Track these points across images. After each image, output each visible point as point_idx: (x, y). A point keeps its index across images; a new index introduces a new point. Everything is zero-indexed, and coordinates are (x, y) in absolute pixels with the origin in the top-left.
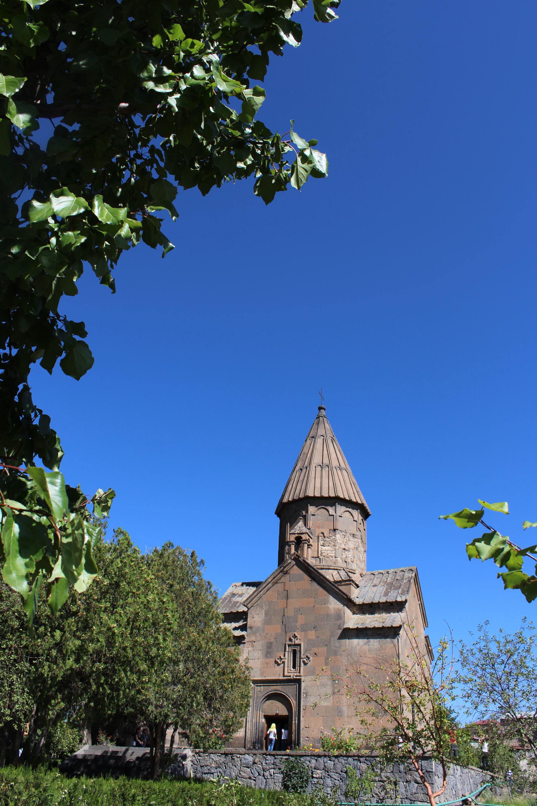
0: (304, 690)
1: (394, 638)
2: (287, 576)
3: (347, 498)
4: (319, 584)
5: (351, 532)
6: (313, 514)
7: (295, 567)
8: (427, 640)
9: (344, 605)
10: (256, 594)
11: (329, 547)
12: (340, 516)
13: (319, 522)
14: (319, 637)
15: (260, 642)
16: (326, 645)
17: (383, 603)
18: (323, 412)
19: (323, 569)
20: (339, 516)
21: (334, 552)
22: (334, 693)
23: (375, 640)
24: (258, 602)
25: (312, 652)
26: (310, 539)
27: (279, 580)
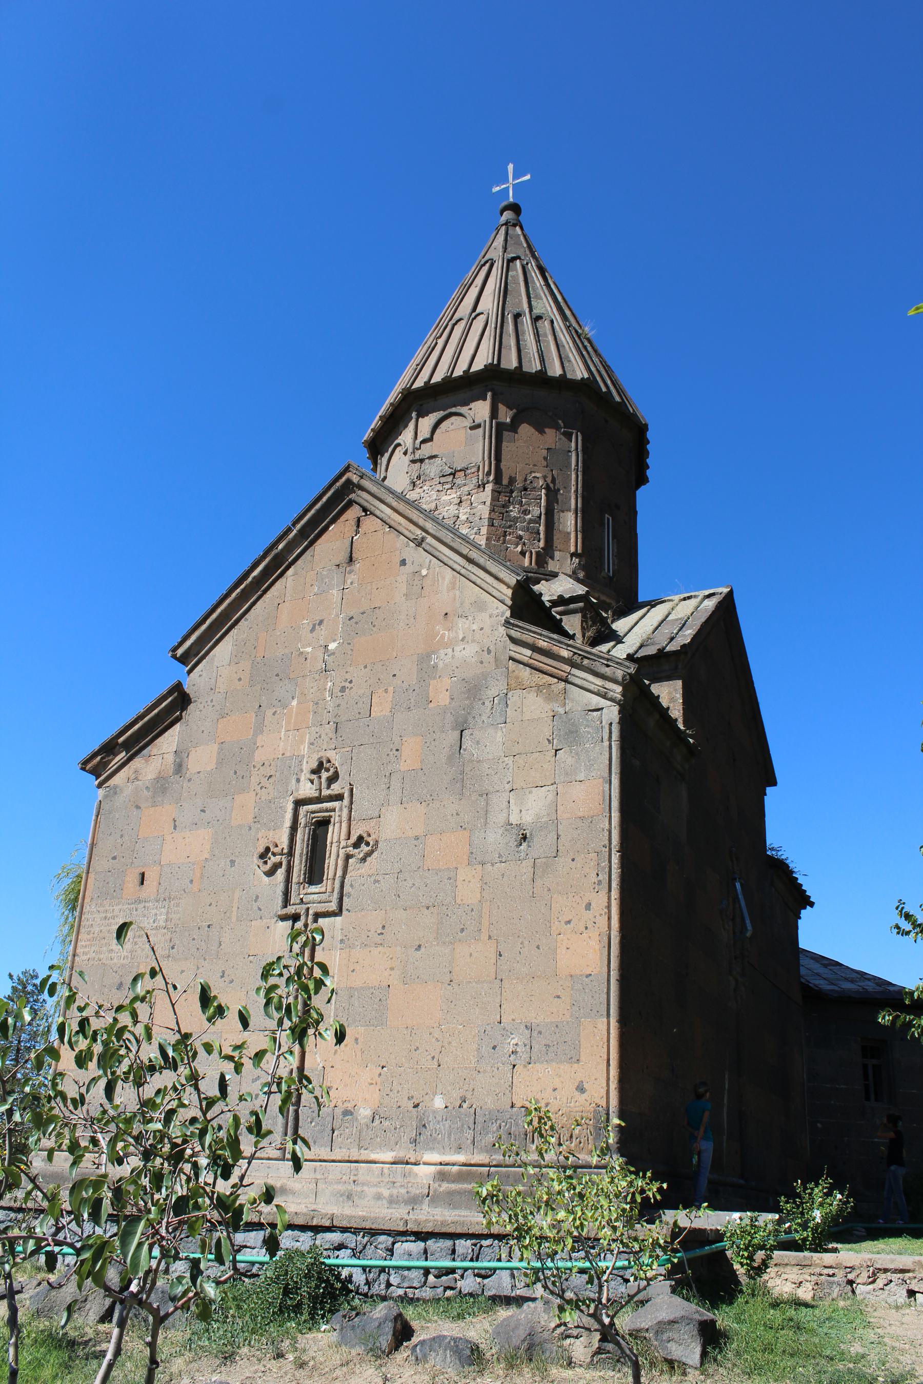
8: (513, 640)
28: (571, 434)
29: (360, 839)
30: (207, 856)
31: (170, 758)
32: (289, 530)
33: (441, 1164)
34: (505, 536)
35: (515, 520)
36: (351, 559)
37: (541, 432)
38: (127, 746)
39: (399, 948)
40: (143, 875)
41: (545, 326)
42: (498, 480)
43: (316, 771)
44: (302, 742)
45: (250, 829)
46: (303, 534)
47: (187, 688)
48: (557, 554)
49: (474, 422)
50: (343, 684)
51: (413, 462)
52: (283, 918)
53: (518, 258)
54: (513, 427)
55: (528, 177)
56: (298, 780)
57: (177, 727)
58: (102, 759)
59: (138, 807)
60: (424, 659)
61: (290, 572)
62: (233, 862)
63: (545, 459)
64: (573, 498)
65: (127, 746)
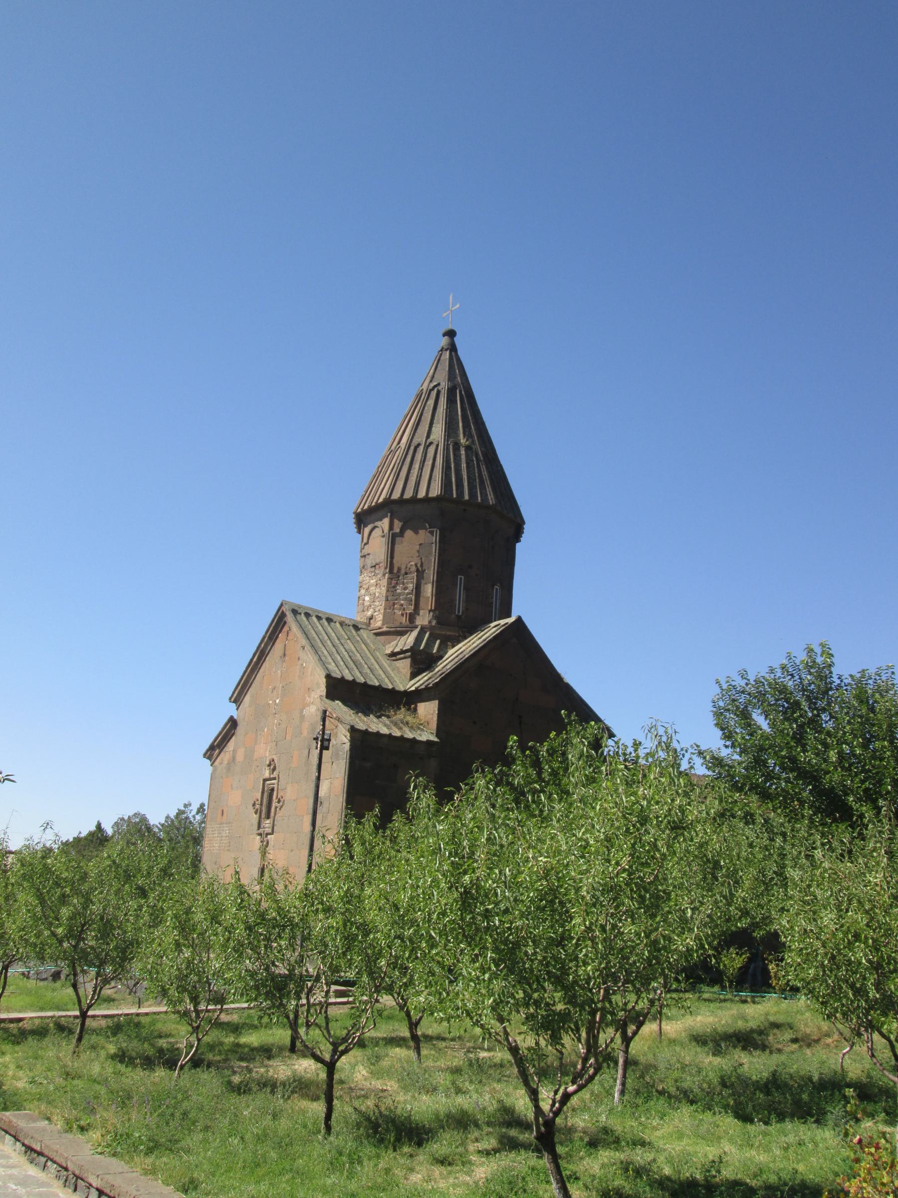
28: (433, 531)
31: (231, 753)
32: (264, 638)
34: (394, 606)
35: (400, 594)
36: (285, 655)
37: (416, 533)
38: (219, 746)
41: (432, 450)
42: (391, 572)
43: (269, 765)
44: (266, 750)
46: (270, 638)
47: (235, 717)
48: (421, 612)
49: (383, 532)
53: (439, 384)
54: (402, 533)
55: (458, 306)
60: (302, 711)
61: (267, 659)
63: (418, 551)
64: (431, 574)
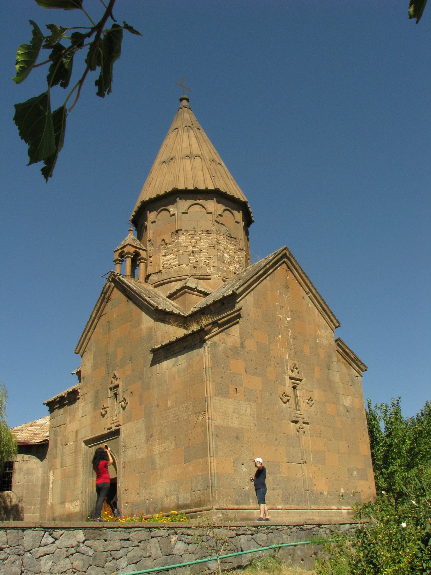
0: (123, 442)
1: (201, 347)
2: (109, 303)
3: (191, 187)
4: (134, 303)
5: (202, 229)
6: (153, 220)
7: (115, 289)
8: (338, 345)
9: (156, 320)
10: (84, 336)
11: (171, 255)
12: (183, 213)
13: (160, 228)
14: (134, 370)
15: (90, 393)
16: (140, 379)
17: (212, 304)
18: (185, 103)
19: (164, 284)
20: (183, 213)
21: (177, 258)
22: (147, 440)
23: (183, 356)
24: (88, 346)
25: (129, 391)
26: (141, 252)
27: (102, 312)
29: (310, 398)
30: (262, 389)
31: (238, 339)
33: (347, 510)
39: (325, 439)
40: (236, 389)
45: (275, 383)
50: (294, 336)
51: (216, 221)
52: (293, 421)
56: (287, 369)
57: (237, 326)
58: (211, 327)
59: (227, 356)
60: (315, 338)
61: (268, 278)
62: (271, 394)
65: (220, 326)
